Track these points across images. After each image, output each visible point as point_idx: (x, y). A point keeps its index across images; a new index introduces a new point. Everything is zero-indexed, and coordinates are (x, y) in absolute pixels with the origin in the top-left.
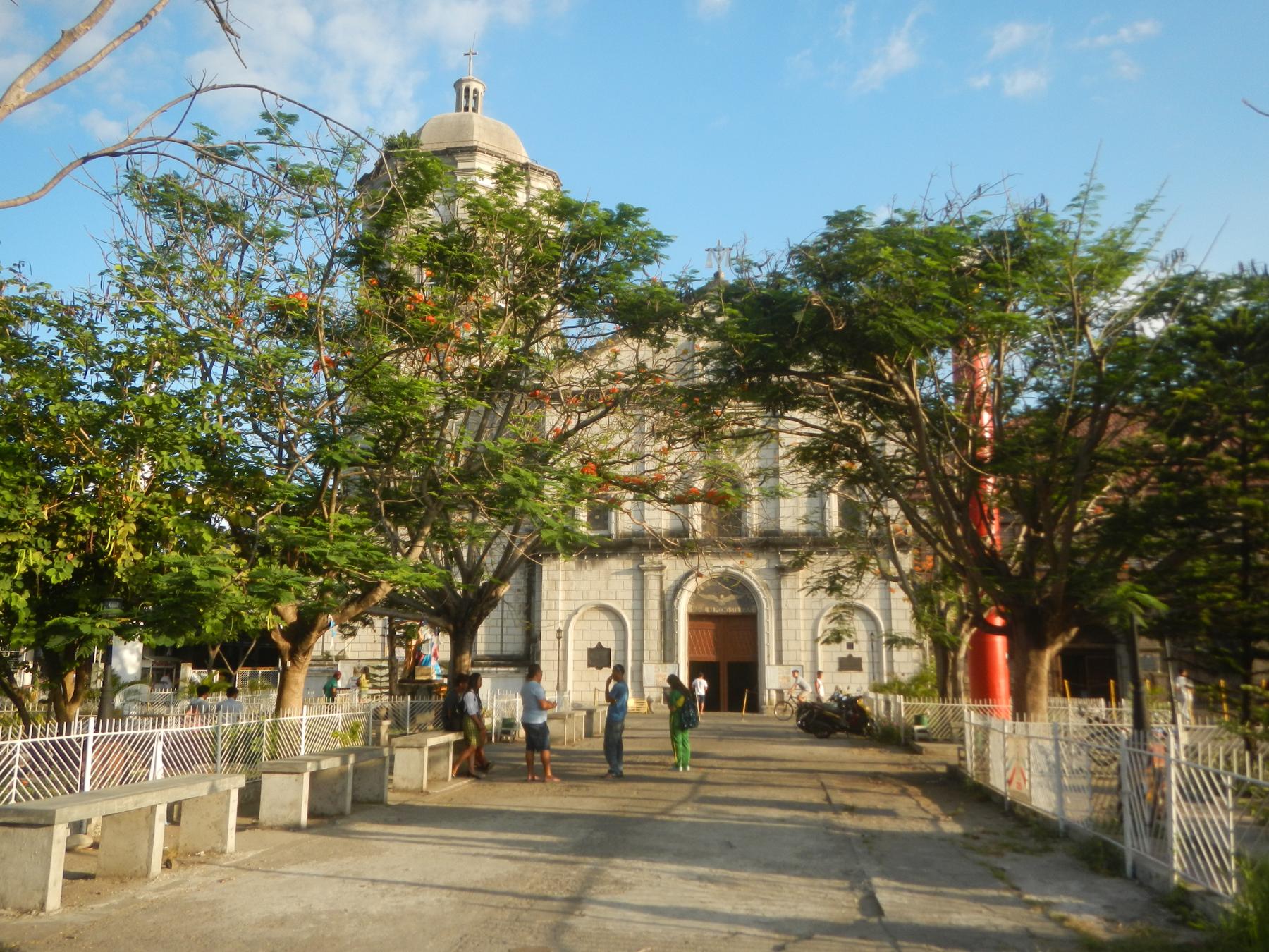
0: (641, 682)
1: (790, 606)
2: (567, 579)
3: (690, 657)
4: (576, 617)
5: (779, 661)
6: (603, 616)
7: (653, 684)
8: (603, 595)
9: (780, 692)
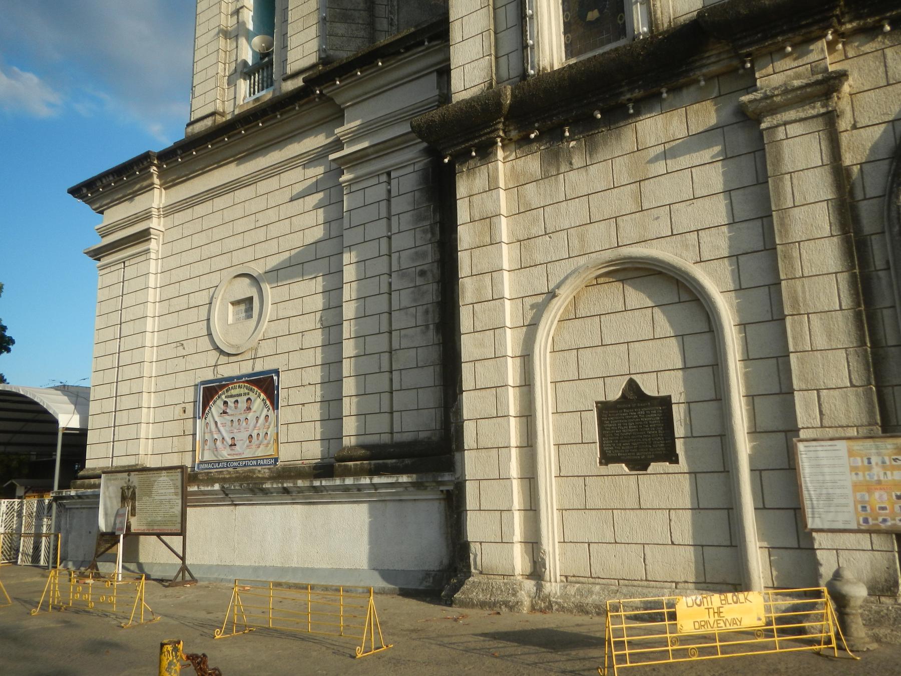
0: (797, 511)
2: (522, 210)
4: (557, 309)
6: (636, 297)
7: (847, 517)
8: (629, 229)
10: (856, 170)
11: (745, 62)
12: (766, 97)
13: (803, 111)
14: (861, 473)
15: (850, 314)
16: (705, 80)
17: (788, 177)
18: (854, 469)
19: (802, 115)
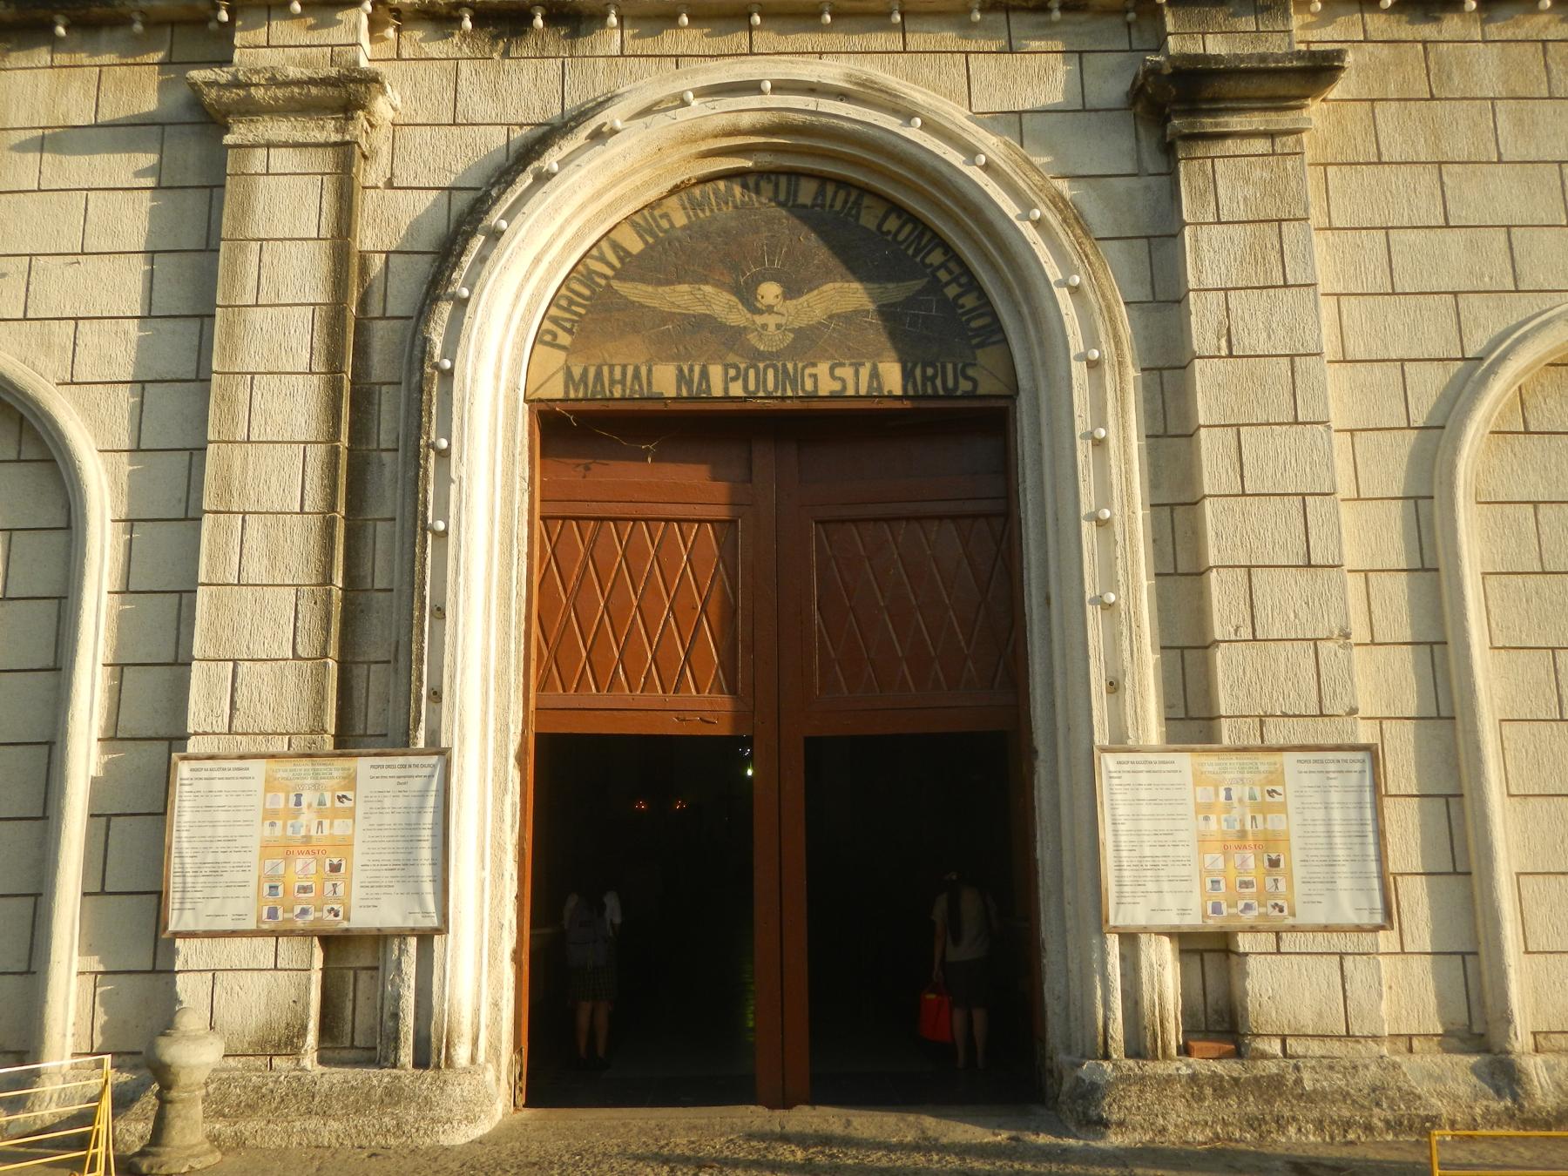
1: (1251, 338)
3: (539, 710)
5: (1193, 718)
7: (242, 908)
9: (1210, 951)
10: (378, 262)
11: (217, 8)
12: (236, 83)
13: (304, 128)
14: (279, 823)
15: (315, 522)
16: (145, 24)
17: (255, 246)
18: (270, 816)
19: (299, 136)
